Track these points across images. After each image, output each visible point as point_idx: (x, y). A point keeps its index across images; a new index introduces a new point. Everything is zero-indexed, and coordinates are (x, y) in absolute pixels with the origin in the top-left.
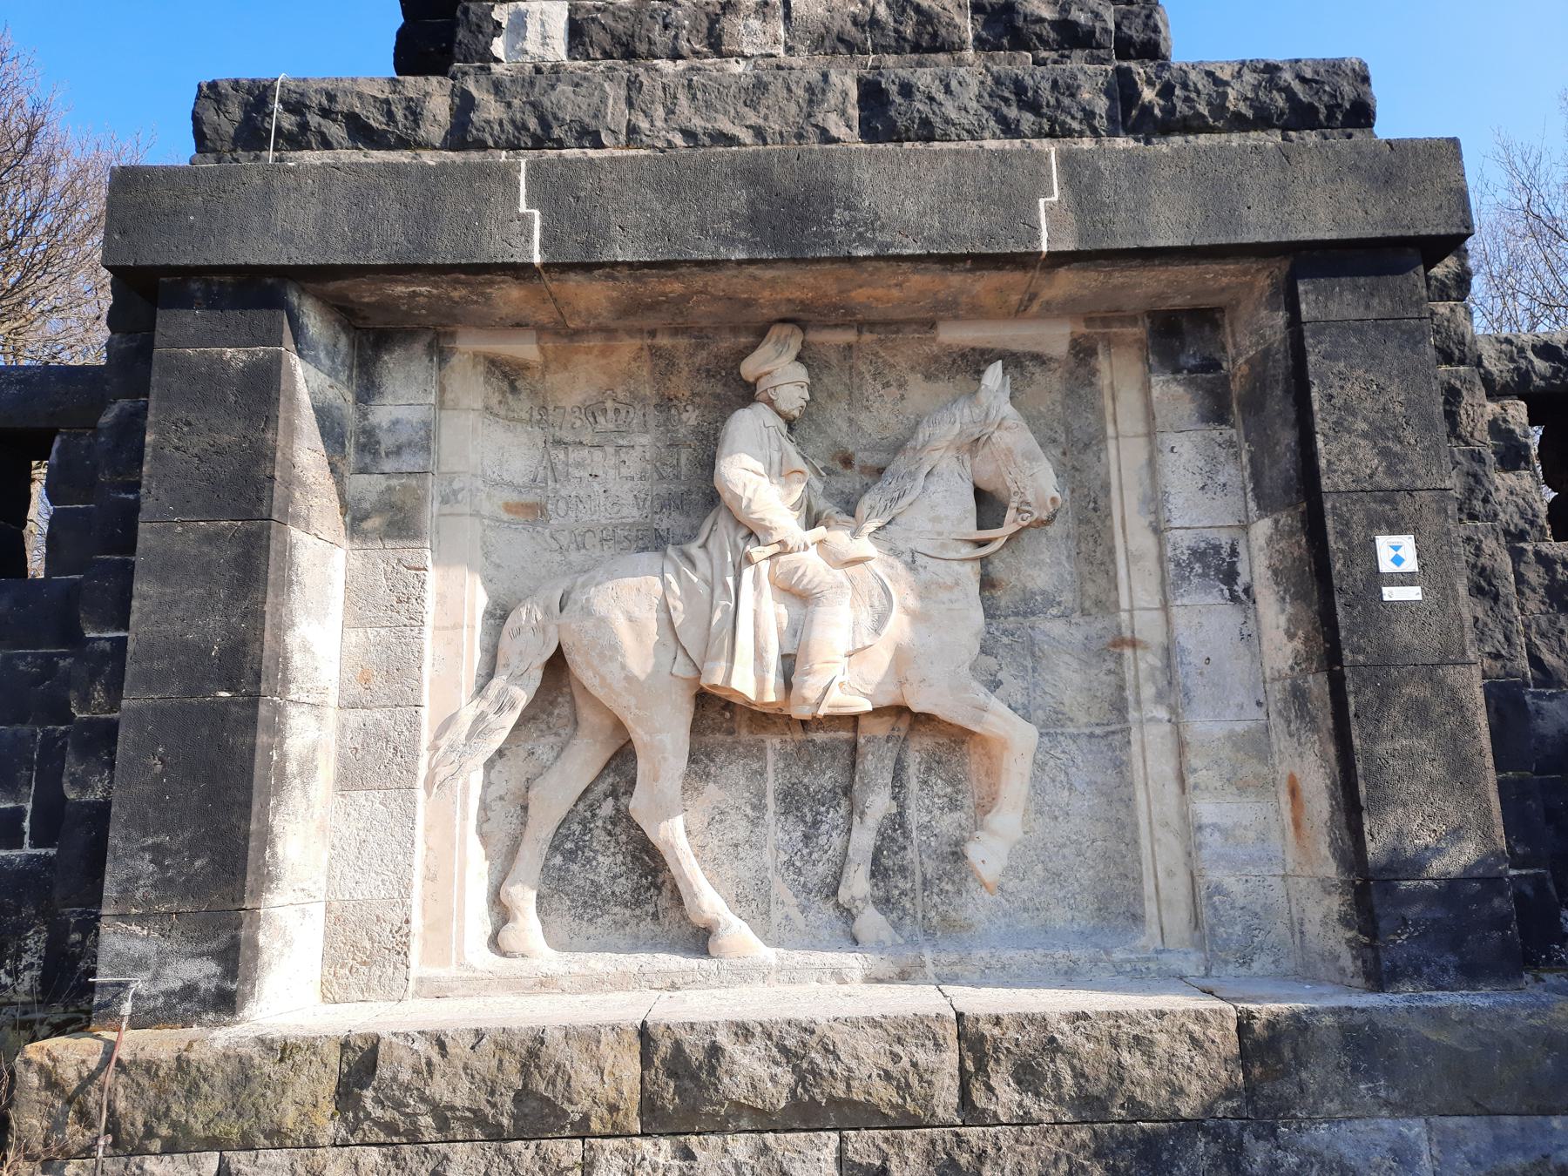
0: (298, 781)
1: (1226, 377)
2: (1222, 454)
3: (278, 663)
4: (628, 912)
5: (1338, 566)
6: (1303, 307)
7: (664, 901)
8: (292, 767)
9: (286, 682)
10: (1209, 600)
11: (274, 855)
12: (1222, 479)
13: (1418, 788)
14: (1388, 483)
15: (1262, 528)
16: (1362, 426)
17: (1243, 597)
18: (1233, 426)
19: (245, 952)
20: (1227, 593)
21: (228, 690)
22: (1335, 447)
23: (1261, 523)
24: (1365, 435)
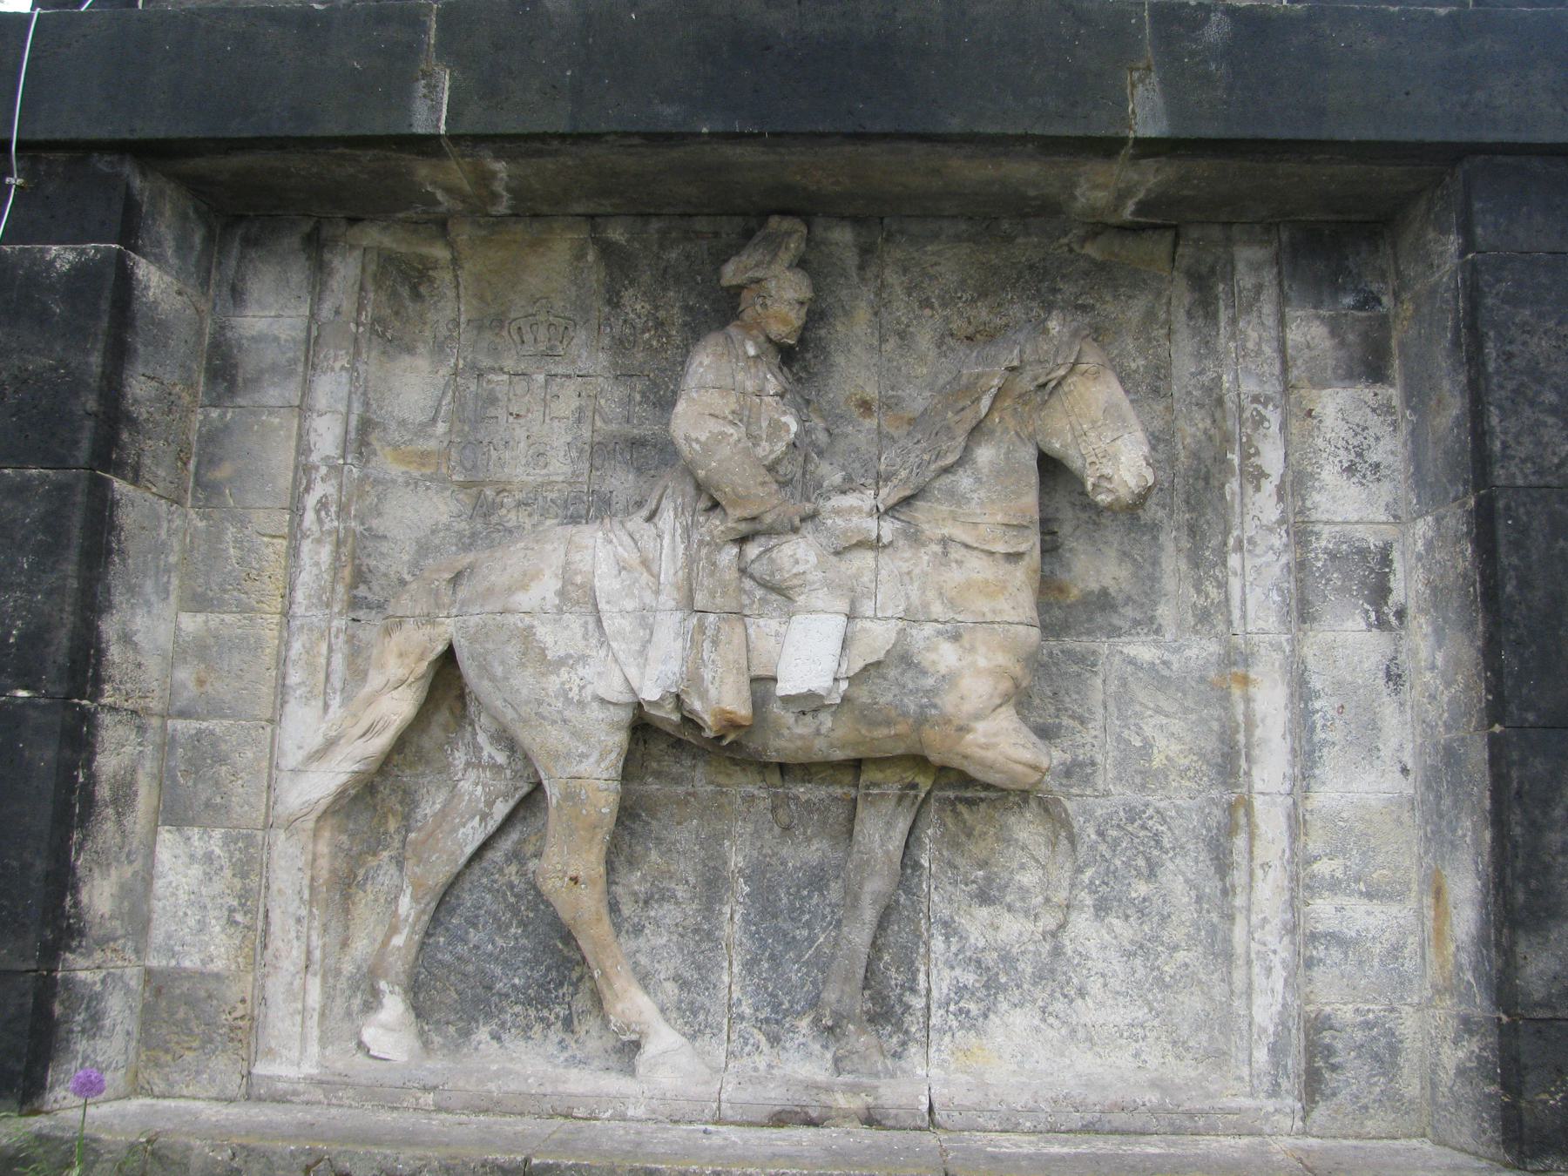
0: (110, 811)
1: (1385, 317)
2: (1374, 420)
3: (88, 655)
4: (532, 1013)
5: (1509, 589)
6: (1479, 231)
7: (582, 1002)
8: (103, 792)
9: (98, 681)
10: (1349, 624)
11: (76, 904)
12: (1375, 459)
15: (1423, 528)
16: (1550, 397)
17: (1393, 619)
18: (1392, 385)
20: (1373, 616)
21: (25, 688)
22: (1513, 424)
23: (1420, 523)
24: (1553, 410)
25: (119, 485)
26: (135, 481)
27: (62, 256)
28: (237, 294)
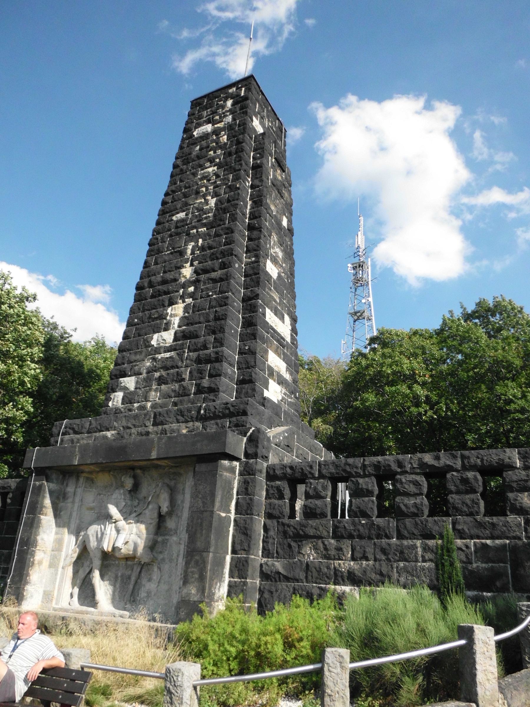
8: (36, 562)
9: (36, 546)
13: (193, 580)
14: (202, 509)
16: (200, 496)
19: (20, 595)
25: (42, 517)
26: (46, 515)
27: (37, 483)
28: (67, 485)
